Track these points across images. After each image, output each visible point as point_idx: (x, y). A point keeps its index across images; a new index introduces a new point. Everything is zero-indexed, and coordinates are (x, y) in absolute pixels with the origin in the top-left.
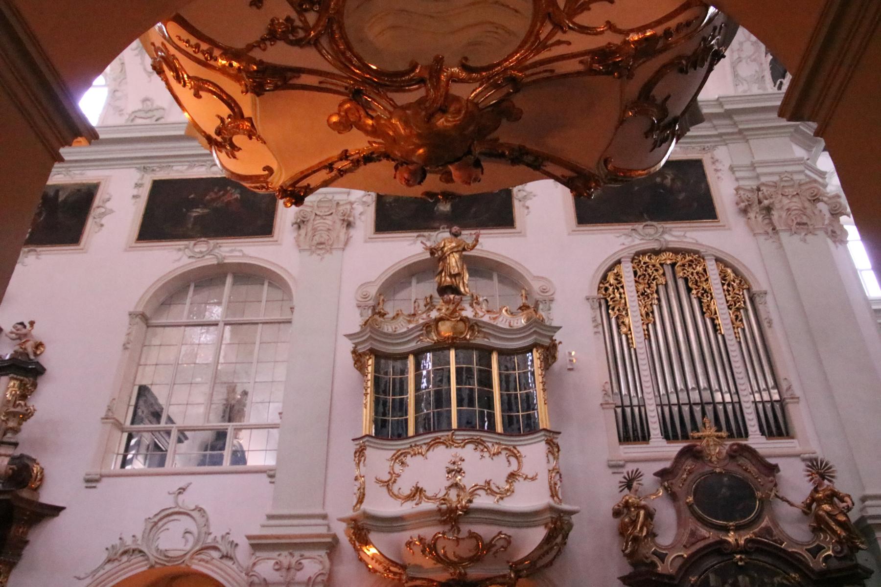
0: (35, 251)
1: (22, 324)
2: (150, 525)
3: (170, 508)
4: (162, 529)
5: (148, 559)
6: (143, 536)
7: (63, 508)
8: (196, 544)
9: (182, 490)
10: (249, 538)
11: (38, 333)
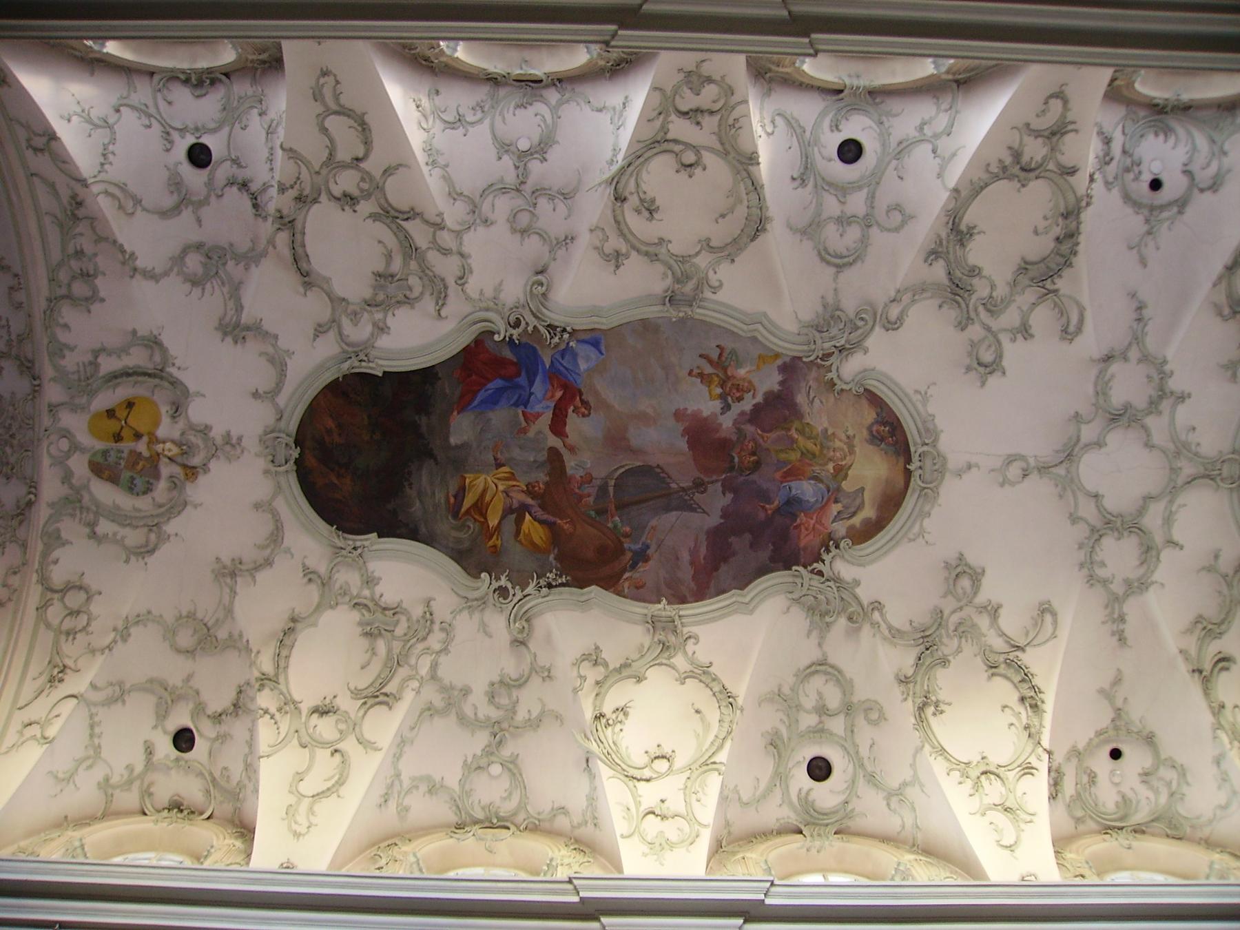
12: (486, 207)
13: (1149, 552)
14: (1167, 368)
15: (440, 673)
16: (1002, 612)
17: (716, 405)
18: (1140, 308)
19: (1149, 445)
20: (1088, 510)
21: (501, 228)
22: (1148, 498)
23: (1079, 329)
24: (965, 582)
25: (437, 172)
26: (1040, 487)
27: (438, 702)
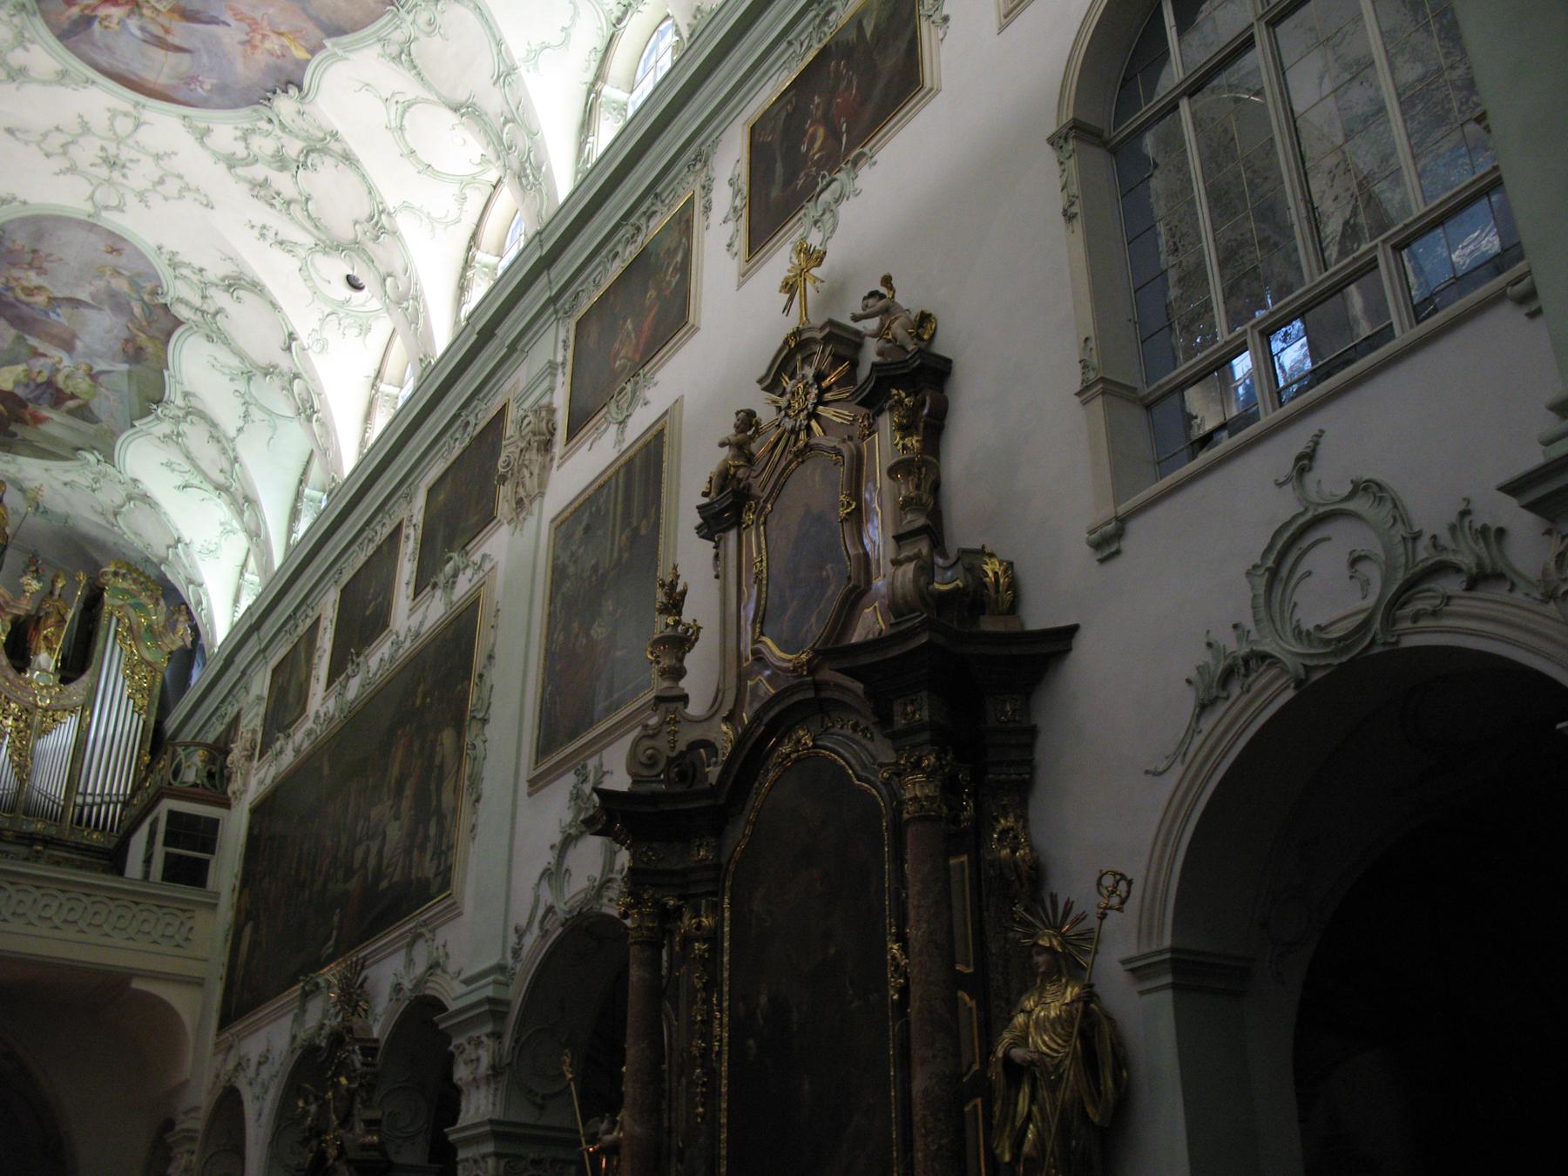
0: (862, 155)
1: (873, 294)
2: (1262, 582)
3: (1295, 518)
4: (1293, 582)
5: (1284, 671)
6: (1255, 615)
7: (1072, 630)
8: (1385, 583)
9: (1305, 462)
10: (1513, 488)
11: (909, 298)
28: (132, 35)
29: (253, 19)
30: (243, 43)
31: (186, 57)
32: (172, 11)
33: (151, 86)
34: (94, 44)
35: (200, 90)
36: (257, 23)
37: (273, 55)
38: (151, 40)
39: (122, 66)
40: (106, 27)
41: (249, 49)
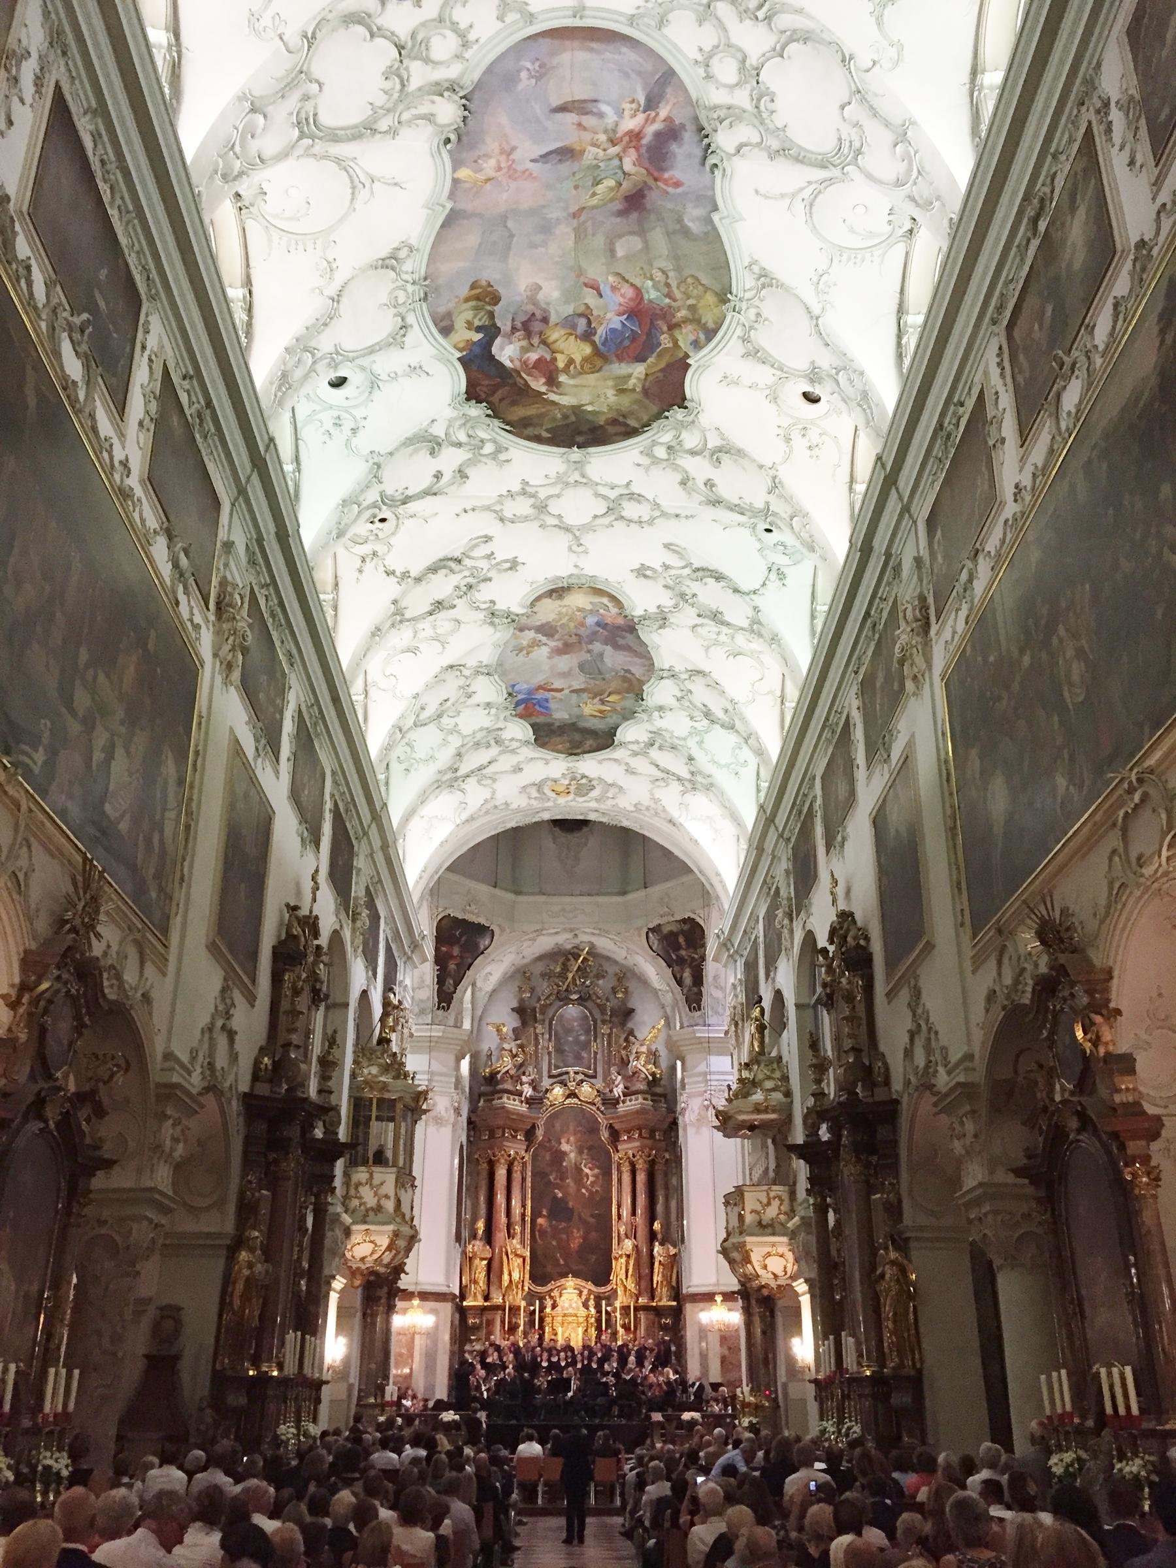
12: (450, 727)
13: (634, 497)
14: (505, 493)
15: (683, 734)
16: (667, 563)
17: (543, 648)
18: (466, 511)
19: (558, 496)
20: (606, 520)
21: (457, 719)
22: (597, 495)
23: (486, 536)
24: (648, 573)
25: (437, 755)
26: (587, 539)
27: (697, 739)
28: (608, 104)
29: (515, 180)
30: (514, 149)
31: (556, 102)
32: (582, 152)
33: (576, 44)
34: (639, 73)
35: (528, 65)
36: (510, 177)
37: (484, 155)
38: (590, 106)
39: (608, 55)
40: (633, 101)
41: (507, 148)
